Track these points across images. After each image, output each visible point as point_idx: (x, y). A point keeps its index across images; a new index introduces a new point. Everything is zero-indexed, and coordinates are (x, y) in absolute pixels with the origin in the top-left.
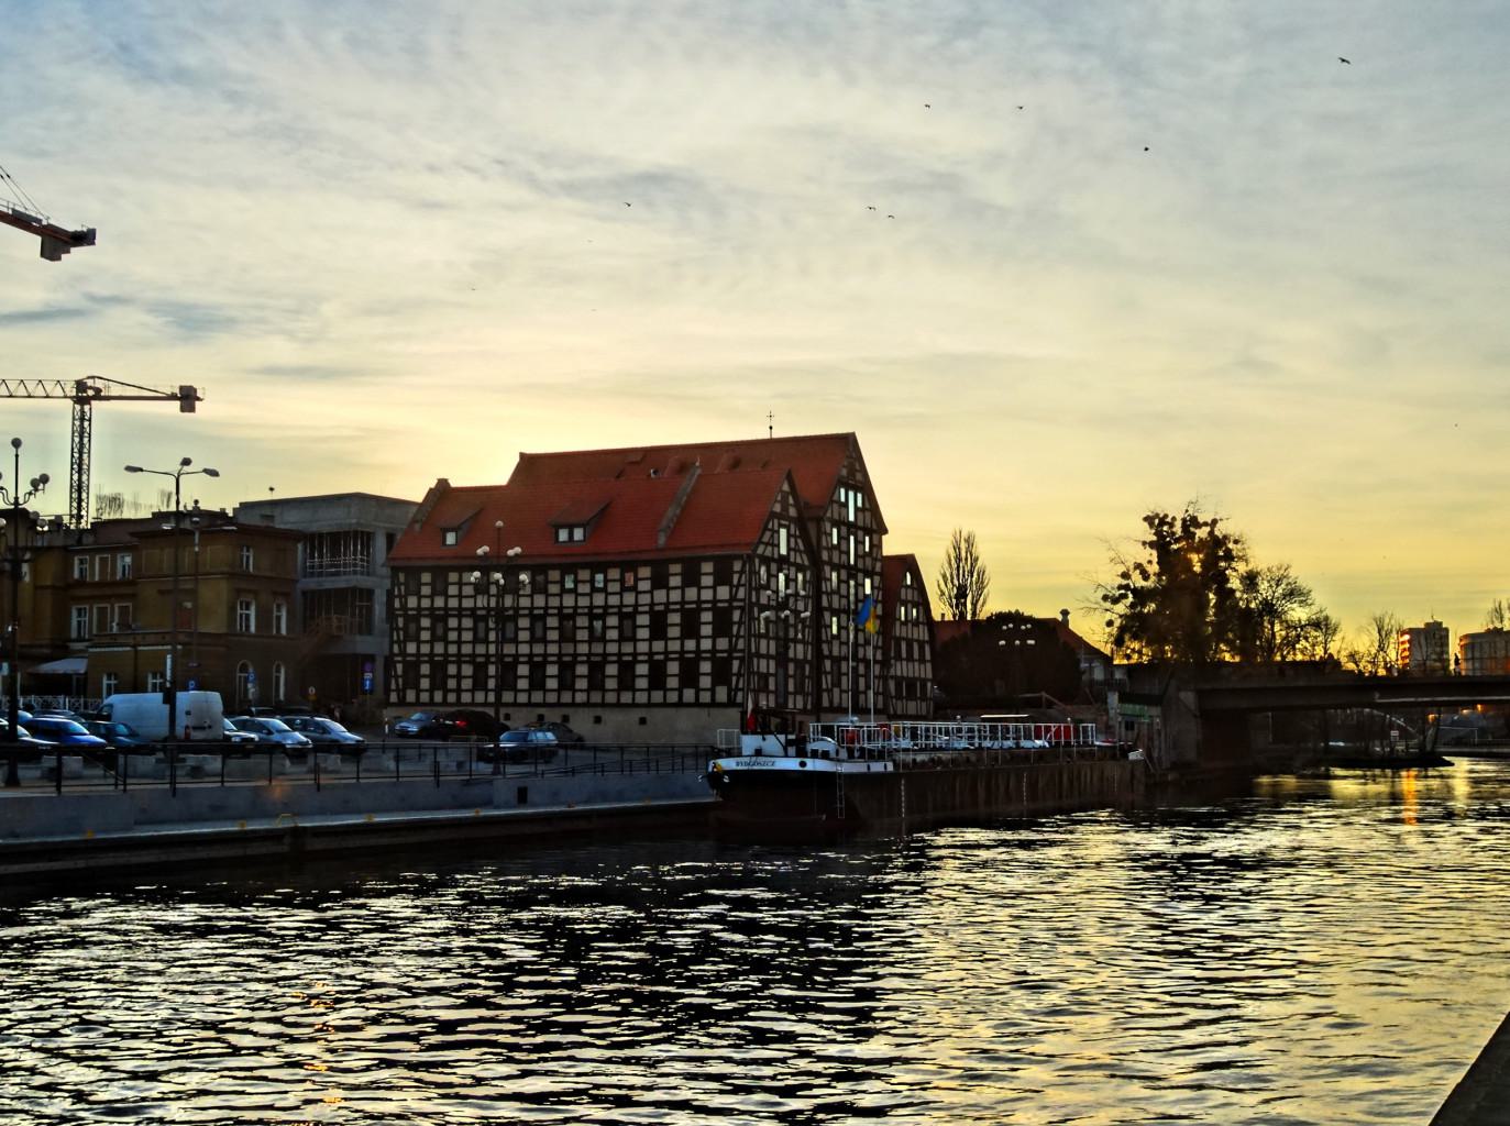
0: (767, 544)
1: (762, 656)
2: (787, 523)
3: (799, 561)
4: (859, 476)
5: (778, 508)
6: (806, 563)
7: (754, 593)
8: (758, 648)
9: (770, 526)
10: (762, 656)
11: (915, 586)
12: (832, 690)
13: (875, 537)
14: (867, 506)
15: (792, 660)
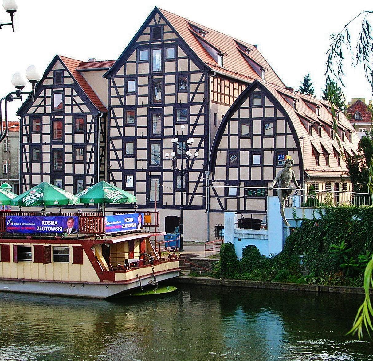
0: (38, 107)
2: (62, 89)
3: (76, 110)
4: (168, 37)
5: (50, 82)
6: (86, 109)
7: (25, 138)
9: (42, 94)
11: (268, 102)
13: (195, 78)
15: (69, 175)
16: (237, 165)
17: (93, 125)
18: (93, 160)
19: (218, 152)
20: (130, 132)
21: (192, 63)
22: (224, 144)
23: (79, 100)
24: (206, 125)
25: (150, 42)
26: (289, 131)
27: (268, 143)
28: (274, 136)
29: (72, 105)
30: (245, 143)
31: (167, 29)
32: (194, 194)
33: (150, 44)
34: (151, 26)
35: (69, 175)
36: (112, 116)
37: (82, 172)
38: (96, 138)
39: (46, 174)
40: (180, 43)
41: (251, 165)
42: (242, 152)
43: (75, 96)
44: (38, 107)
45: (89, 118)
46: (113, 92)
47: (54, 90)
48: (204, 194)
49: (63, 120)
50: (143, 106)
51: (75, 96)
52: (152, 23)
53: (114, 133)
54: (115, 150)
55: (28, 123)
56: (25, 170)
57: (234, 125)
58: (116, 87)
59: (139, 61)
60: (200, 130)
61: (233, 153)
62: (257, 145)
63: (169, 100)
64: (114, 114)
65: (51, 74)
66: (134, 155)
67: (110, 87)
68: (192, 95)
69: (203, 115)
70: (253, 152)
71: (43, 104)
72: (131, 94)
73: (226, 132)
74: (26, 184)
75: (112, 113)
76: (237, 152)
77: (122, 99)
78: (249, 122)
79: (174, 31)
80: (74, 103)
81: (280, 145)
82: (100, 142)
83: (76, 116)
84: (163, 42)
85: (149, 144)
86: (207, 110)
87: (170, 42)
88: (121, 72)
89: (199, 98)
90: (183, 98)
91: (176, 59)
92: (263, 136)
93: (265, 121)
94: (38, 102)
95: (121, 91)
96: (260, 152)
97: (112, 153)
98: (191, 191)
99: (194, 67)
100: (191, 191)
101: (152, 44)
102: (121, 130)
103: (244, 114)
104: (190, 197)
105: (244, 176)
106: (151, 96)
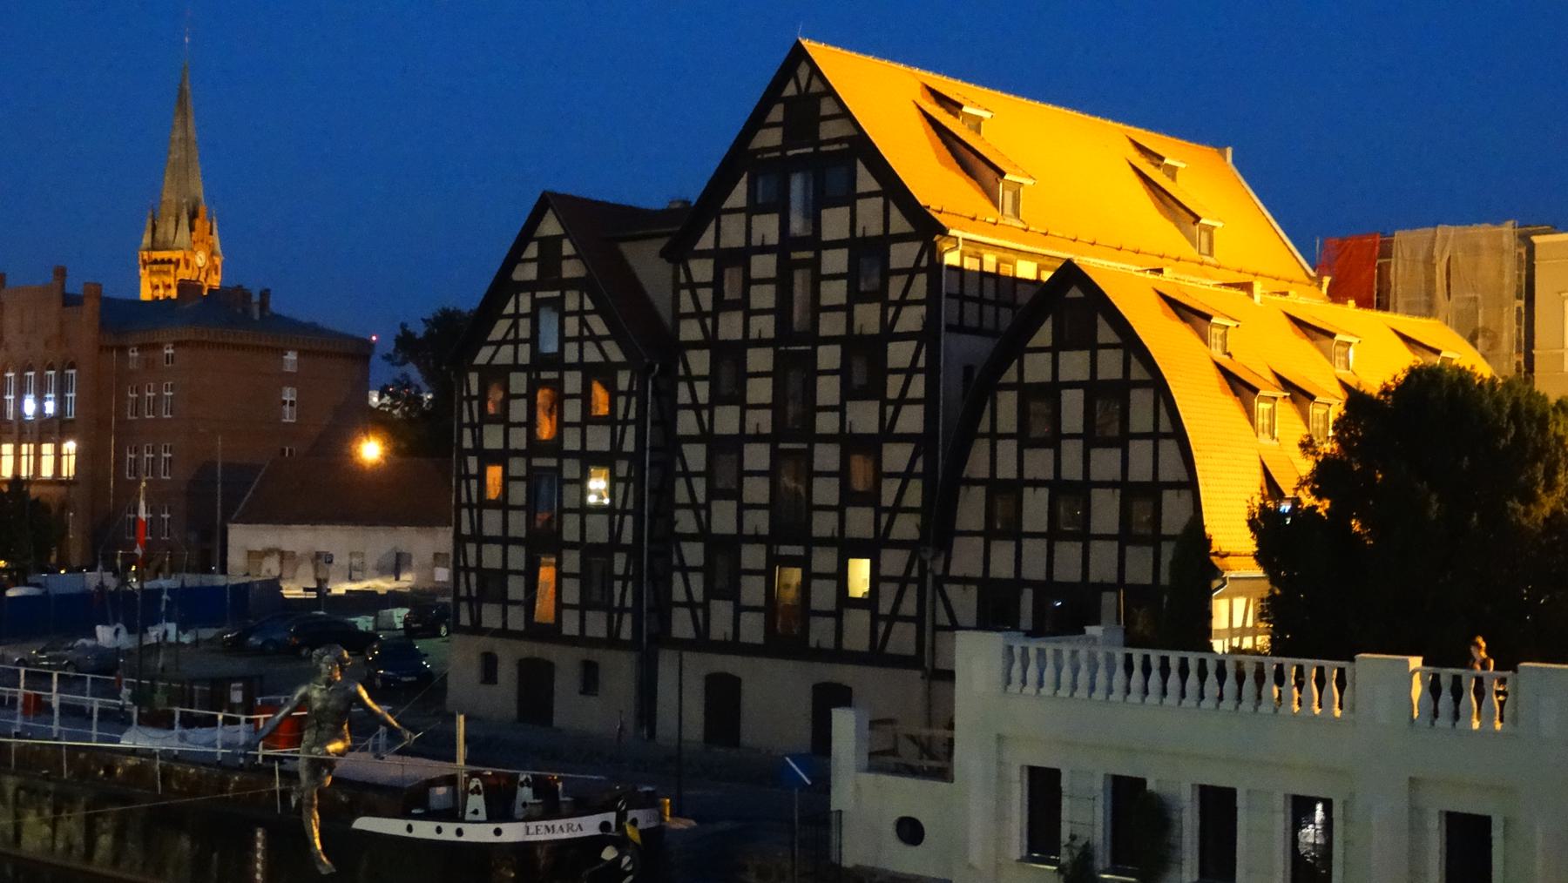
0: (499, 344)
1: (492, 540)
2: (557, 294)
3: (592, 355)
5: (527, 272)
6: (616, 355)
8: (478, 526)
9: (510, 309)
10: (492, 540)
11: (1105, 333)
12: (705, 606)
13: (903, 255)
14: (866, 181)
15: (572, 546)
16: (1015, 533)
17: (634, 400)
18: (630, 505)
19: (963, 489)
20: (727, 421)
21: (895, 213)
22: (978, 465)
23: (598, 326)
24: (930, 401)
25: (782, 148)
26: (1165, 425)
27: (1106, 463)
28: (1122, 440)
29: (580, 339)
30: (1039, 464)
31: (827, 107)
32: (894, 616)
33: (784, 153)
34: (788, 102)
35: (572, 546)
36: (681, 372)
37: (603, 538)
38: (640, 438)
39: (517, 541)
40: (862, 147)
41: (1053, 535)
42: (1028, 491)
43: (590, 312)
44: (499, 344)
45: (623, 380)
46: (686, 304)
47: (539, 295)
48: (918, 620)
49: (557, 386)
50: (761, 343)
51: (590, 312)
52: (790, 90)
53: (687, 423)
54: (688, 476)
55: (475, 390)
56: (466, 529)
57: (1007, 403)
58: (693, 286)
59: (753, 208)
60: (911, 420)
61: (1005, 494)
62: (1072, 470)
63: (831, 325)
64: (686, 366)
65: (532, 251)
66: (736, 494)
67: (677, 288)
68: (891, 311)
69: (920, 371)
70: (1058, 487)
71: (511, 336)
72: (732, 306)
73: (984, 426)
74: (467, 570)
75: (681, 367)
76: (1016, 487)
77: (709, 322)
78: (1052, 390)
79: (845, 114)
80: (586, 333)
81: (1140, 470)
82: (653, 449)
83: (590, 372)
84: (816, 150)
85: (776, 455)
86: (933, 358)
87: (836, 147)
88: (706, 241)
89: (911, 319)
90: (868, 318)
91: (850, 198)
92: (1091, 438)
93: (1094, 389)
94: (500, 329)
95: (706, 296)
96: (1083, 489)
97: (680, 486)
98: (885, 608)
99: (899, 223)
100: (885, 608)
101: (790, 153)
102: (705, 415)
103: (1037, 368)
104: (882, 627)
105: (1034, 569)
106: (782, 311)
